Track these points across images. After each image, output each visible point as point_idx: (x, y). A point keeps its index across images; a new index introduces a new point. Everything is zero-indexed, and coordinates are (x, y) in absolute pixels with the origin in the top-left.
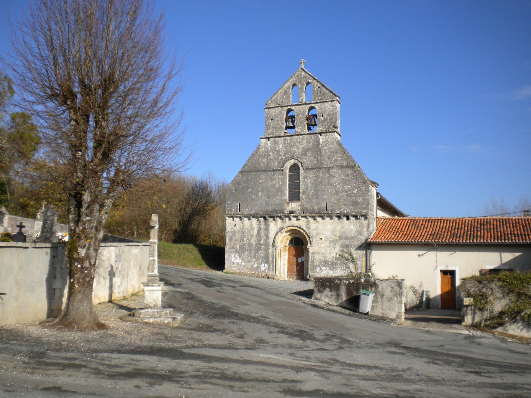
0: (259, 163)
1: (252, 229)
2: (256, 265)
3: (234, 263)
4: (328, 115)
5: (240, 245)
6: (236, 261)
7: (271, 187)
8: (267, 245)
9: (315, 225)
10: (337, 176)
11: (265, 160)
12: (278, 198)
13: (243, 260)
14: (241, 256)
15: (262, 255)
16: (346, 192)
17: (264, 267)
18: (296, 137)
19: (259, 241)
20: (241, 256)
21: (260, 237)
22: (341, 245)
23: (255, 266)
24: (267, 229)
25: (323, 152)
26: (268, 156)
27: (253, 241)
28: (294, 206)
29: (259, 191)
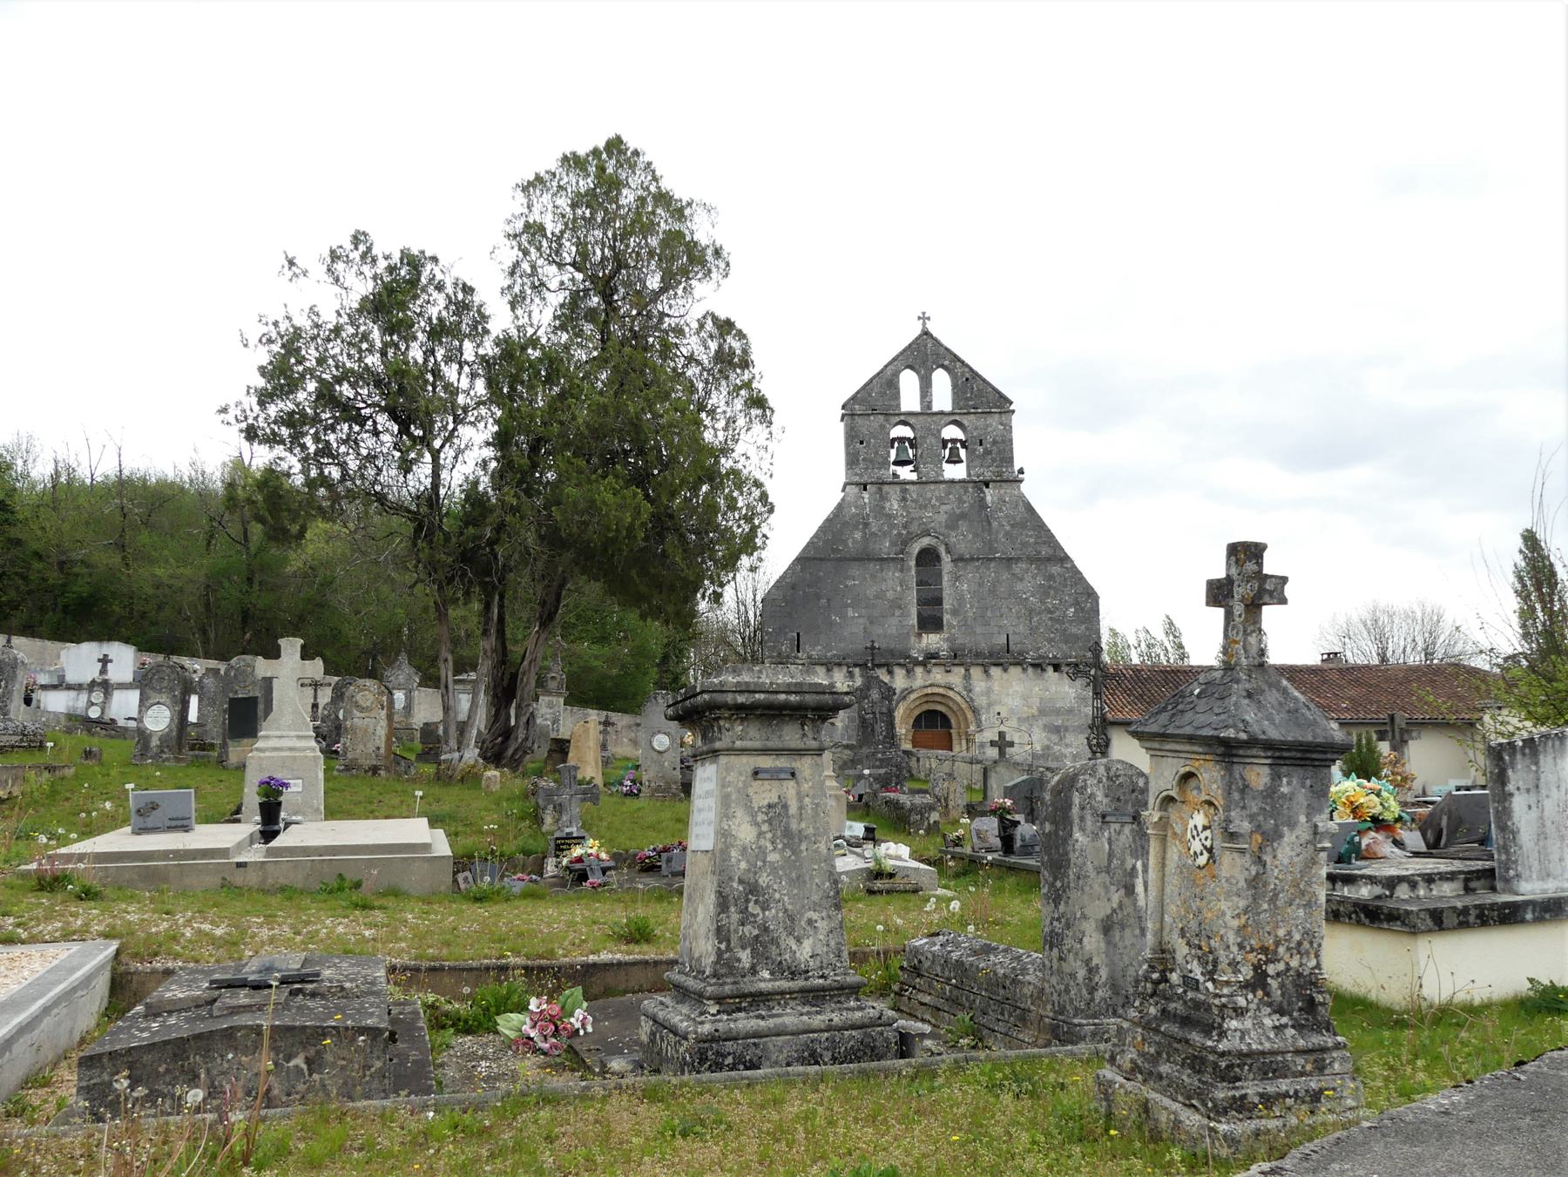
0: (844, 542)
4: (995, 442)
7: (877, 597)
9: (983, 684)
10: (1028, 577)
11: (858, 535)
16: (1050, 612)
18: (932, 487)
22: (1045, 726)
25: (995, 524)
26: (866, 525)
28: (932, 641)
29: (847, 606)
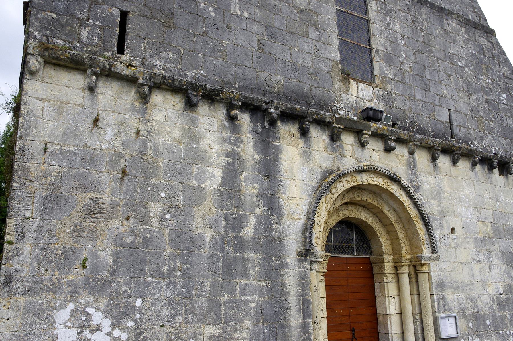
1: (197, 157)
5: (118, 240)
8: (271, 244)
12: (308, 46)
14: (128, 311)
15: (253, 301)
19: (237, 223)
20: (128, 311)
21: (240, 205)
24: (269, 170)
27: (205, 224)
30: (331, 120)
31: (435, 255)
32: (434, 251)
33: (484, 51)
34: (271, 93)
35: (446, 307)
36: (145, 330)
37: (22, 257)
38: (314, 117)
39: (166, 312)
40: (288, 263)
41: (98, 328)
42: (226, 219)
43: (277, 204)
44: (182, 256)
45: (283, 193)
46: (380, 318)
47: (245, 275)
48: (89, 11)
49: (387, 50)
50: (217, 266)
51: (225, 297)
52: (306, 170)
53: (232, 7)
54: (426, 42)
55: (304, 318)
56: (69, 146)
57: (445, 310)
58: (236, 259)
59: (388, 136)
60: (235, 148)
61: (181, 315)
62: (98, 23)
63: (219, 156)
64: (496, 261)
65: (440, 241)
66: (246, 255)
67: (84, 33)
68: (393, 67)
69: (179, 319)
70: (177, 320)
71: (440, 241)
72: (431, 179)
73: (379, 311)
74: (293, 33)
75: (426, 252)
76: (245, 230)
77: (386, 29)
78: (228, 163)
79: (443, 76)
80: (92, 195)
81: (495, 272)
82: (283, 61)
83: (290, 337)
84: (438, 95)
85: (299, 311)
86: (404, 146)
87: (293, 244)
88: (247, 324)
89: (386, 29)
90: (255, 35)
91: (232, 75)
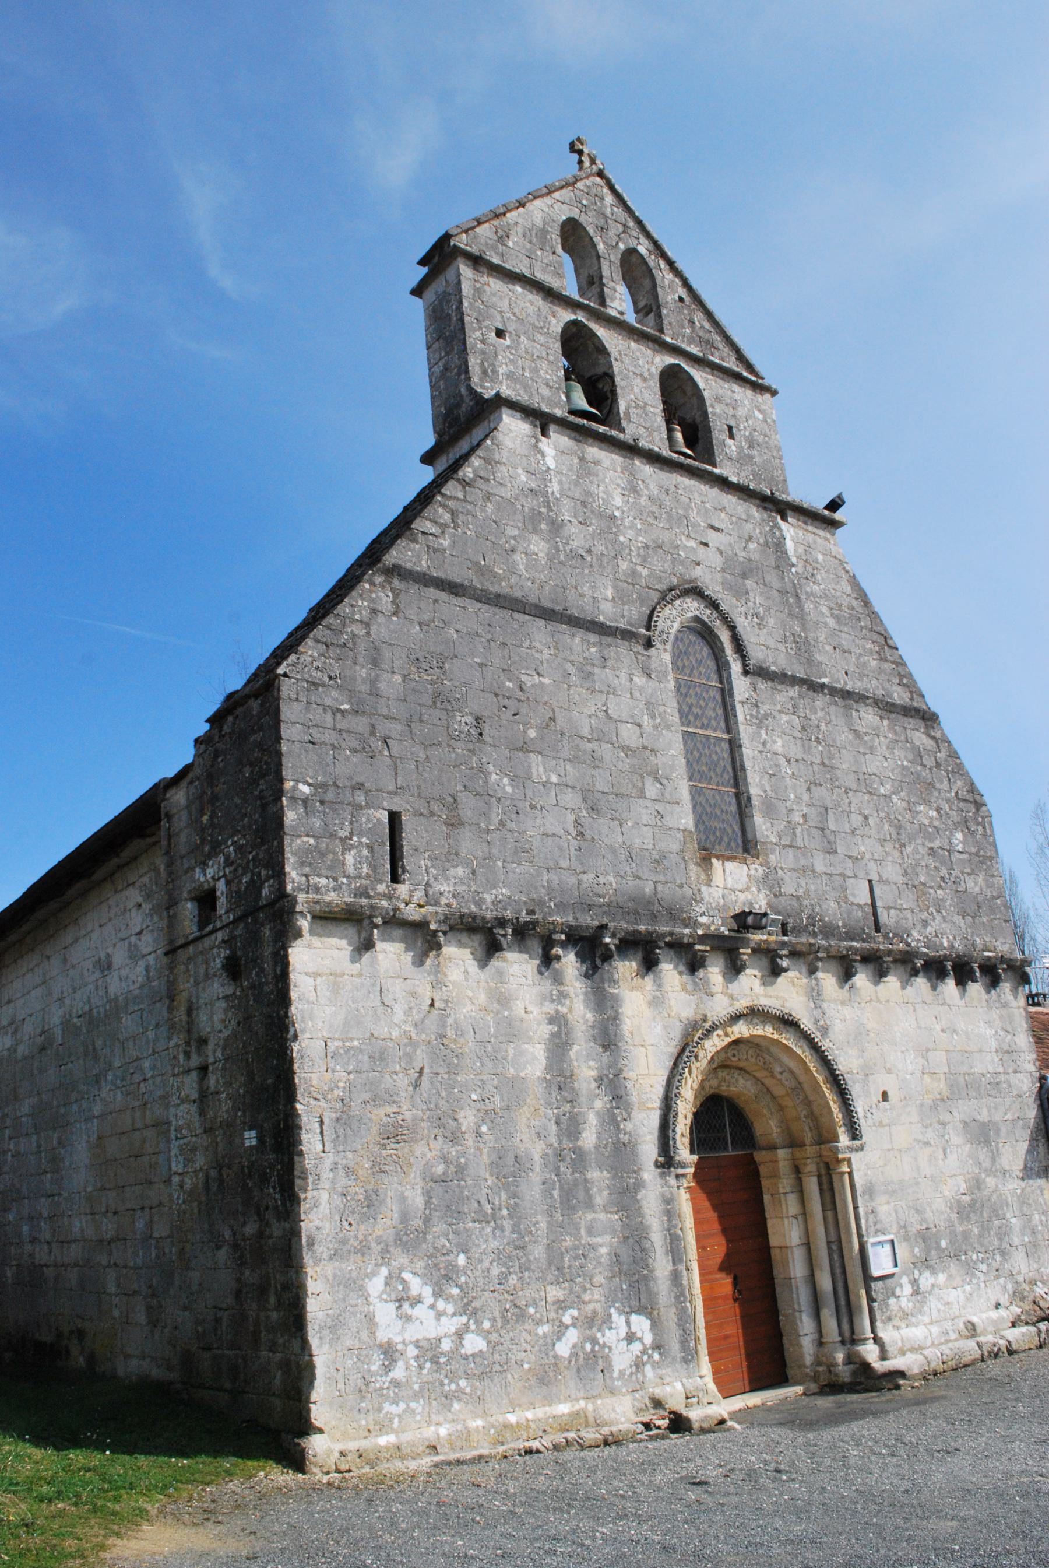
2: (572, 1335)
3: (390, 1353)
6: (414, 1332)
8: (620, 1154)
13: (467, 1308)
15: (605, 1244)
17: (631, 1338)
19: (571, 1127)
23: (563, 1349)
24: (608, 1037)
27: (532, 1135)
30: (691, 940)
31: (857, 1143)
32: (854, 1134)
33: (921, 757)
34: (600, 906)
35: (878, 1226)
36: (474, 1298)
37: (322, 1208)
38: (667, 940)
39: (495, 1271)
40: (645, 1181)
41: (417, 1301)
42: (557, 1123)
43: (623, 1089)
44: (506, 1187)
45: (629, 1070)
46: (775, 1254)
47: (589, 1205)
48: (351, 823)
49: (765, 791)
50: (552, 1197)
51: (569, 1241)
52: (659, 1029)
53: (534, 770)
54: (827, 762)
55: (674, 1263)
56: (352, 1039)
57: (877, 1231)
58: (576, 1183)
59: (776, 950)
60: (559, 1007)
61: (515, 1273)
62: (364, 840)
63: (539, 1024)
64: (956, 1139)
65: (866, 1117)
66: (589, 1176)
67: (350, 859)
68: (775, 822)
69: (513, 1280)
70: (510, 1281)
71: (866, 1117)
72: (847, 1012)
73: (774, 1241)
74: (622, 796)
75: (844, 1140)
76: (584, 1135)
77: (761, 752)
78: (553, 1034)
79: (856, 820)
80: (390, 1109)
81: (952, 1160)
82: (611, 848)
83: (657, 1294)
84: (850, 857)
85: (667, 1254)
86: (801, 961)
87: (649, 1150)
88: (599, 1279)
89: (761, 752)
90: (569, 811)
91: (544, 887)
